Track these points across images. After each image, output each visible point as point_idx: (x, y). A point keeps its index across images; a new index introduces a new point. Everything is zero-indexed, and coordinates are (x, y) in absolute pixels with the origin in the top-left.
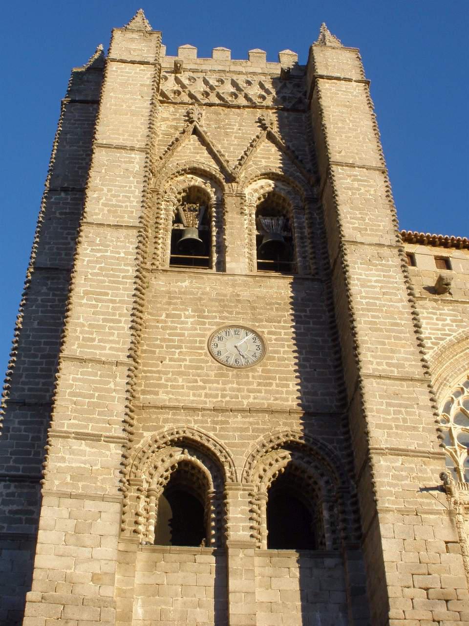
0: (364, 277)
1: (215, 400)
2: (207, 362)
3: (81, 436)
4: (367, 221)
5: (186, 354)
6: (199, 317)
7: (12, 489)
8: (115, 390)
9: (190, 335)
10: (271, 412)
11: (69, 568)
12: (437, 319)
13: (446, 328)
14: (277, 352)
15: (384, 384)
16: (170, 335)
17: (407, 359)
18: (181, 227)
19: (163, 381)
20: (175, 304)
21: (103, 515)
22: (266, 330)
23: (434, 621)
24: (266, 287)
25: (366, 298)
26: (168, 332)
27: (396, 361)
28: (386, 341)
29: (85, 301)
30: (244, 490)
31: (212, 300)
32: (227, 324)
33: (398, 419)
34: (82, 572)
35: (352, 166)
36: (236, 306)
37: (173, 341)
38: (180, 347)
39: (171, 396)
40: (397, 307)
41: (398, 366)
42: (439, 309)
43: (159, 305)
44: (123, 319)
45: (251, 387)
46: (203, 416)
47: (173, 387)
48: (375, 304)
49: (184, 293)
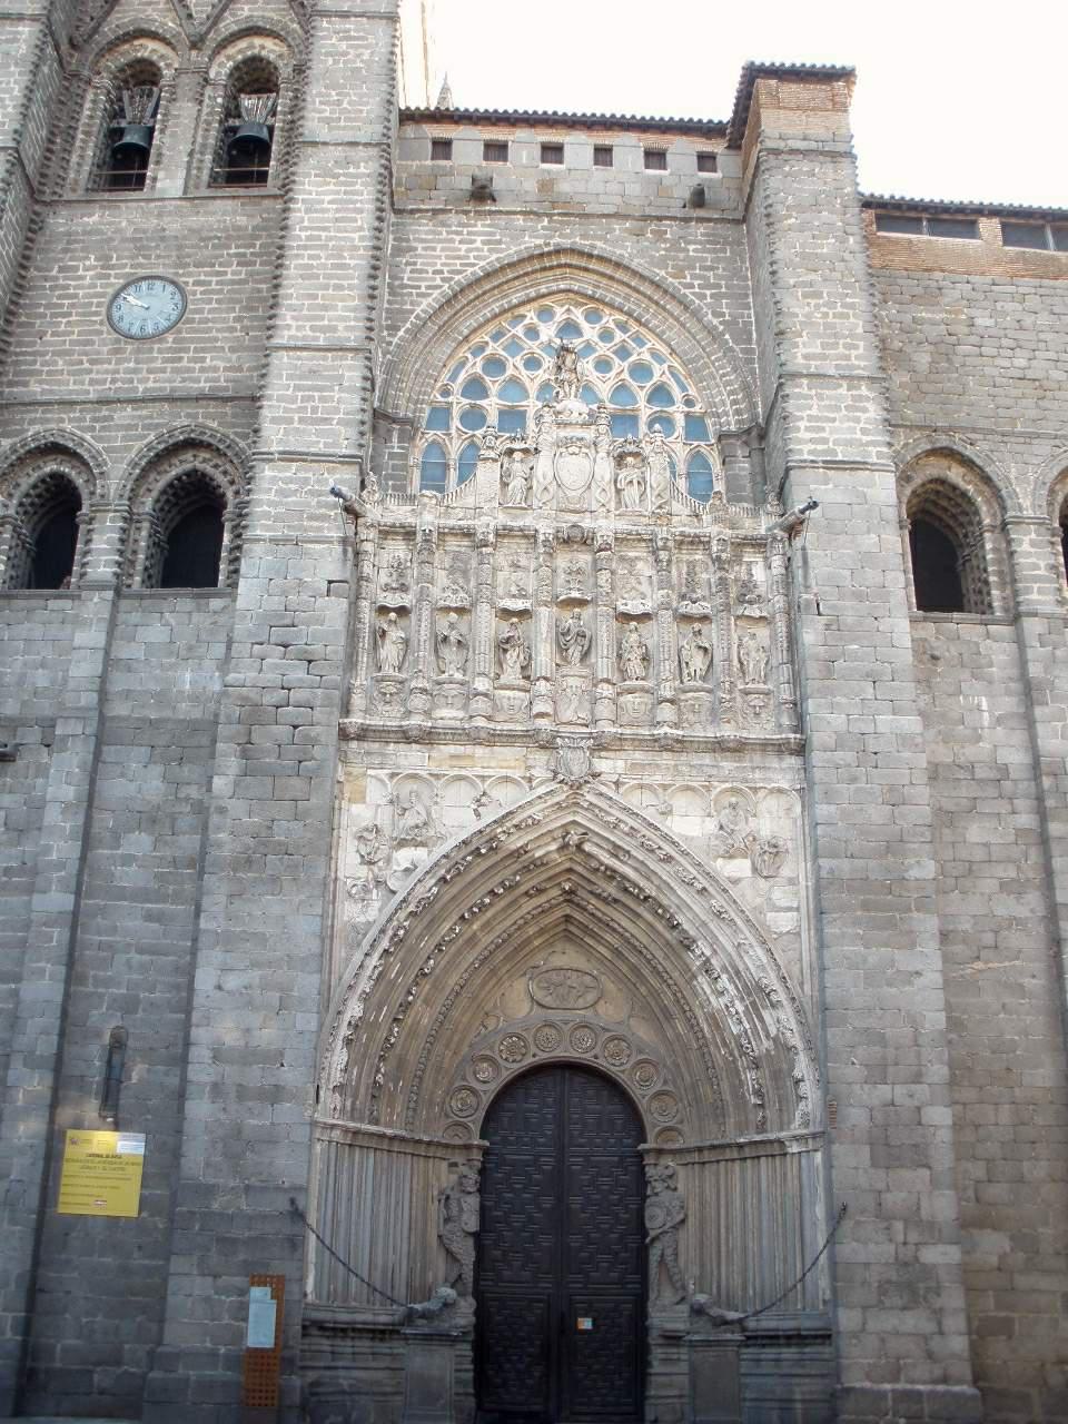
0: (314, 196)
1: (100, 388)
2: (101, 333)
4: (345, 105)
5: (78, 323)
6: (103, 267)
9: (85, 296)
10: (171, 399)
12: (460, 242)
13: (471, 255)
14: (200, 311)
15: (299, 358)
16: (59, 297)
18: (124, 124)
19: (38, 367)
20: (74, 250)
22: (191, 280)
23: (283, 688)
24: (207, 213)
25: (307, 229)
26: (57, 293)
27: (326, 322)
28: (320, 293)
30: (116, 511)
31: (124, 240)
32: (140, 275)
33: (306, 408)
35: (345, 15)
36: (157, 247)
37: (62, 306)
38: (65, 315)
39: (46, 387)
40: (353, 240)
41: (323, 329)
42: (464, 225)
43: (52, 255)
45: (153, 365)
46: (81, 411)
47: (49, 373)
48: (319, 238)
49: (89, 233)
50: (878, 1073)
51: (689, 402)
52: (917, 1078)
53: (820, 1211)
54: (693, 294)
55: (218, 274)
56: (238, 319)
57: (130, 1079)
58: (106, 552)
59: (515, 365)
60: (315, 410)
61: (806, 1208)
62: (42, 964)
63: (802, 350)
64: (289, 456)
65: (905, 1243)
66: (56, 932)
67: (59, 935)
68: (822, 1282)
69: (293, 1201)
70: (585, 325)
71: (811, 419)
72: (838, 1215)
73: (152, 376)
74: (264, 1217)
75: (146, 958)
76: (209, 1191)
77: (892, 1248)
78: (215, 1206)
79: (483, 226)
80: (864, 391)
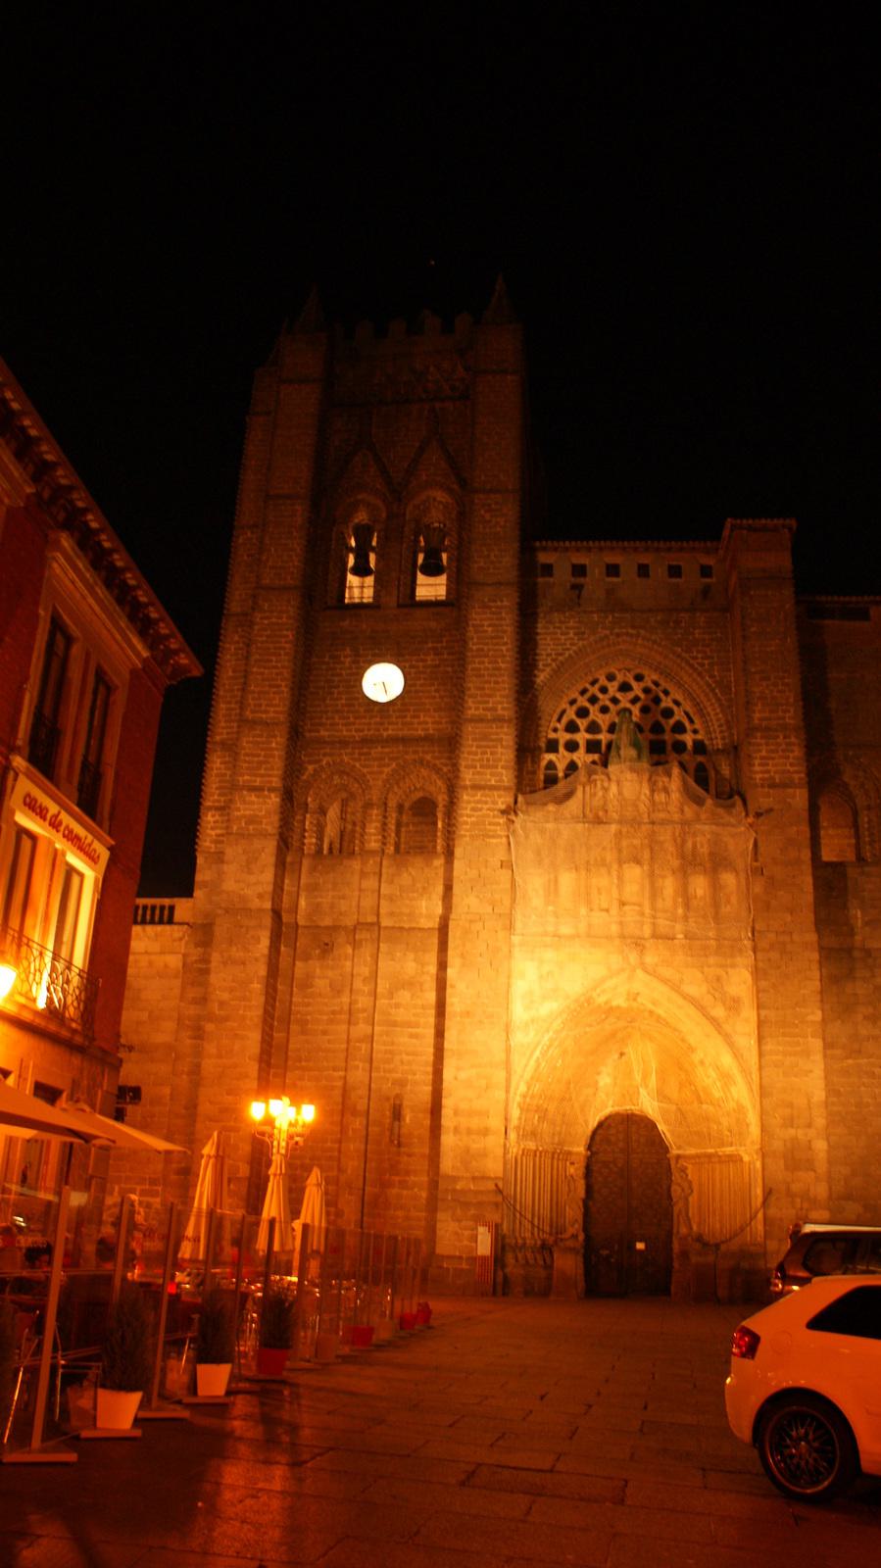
0: (479, 622)
1: (361, 734)
3: (253, 789)
6: (355, 656)
7: (217, 817)
8: (277, 749)
11: (243, 889)
12: (561, 634)
13: (568, 642)
17: (502, 703)
21: (266, 850)
26: (330, 673)
27: (491, 705)
28: (486, 686)
29: (255, 670)
34: (248, 892)
44: (283, 684)
47: (331, 725)
48: (483, 650)
50: (790, 1122)
51: (695, 732)
52: (809, 1126)
53: (759, 1191)
54: (698, 663)
55: (422, 660)
56: (436, 691)
57: (404, 1120)
58: (375, 835)
59: (594, 710)
60: (488, 760)
61: (753, 1189)
62: (356, 1063)
63: (757, 715)
64: (476, 787)
65: (801, 1209)
66: (364, 1046)
67: (364, 1047)
68: (759, 1226)
69: (496, 1185)
70: (634, 684)
71: (762, 758)
72: (768, 1194)
73: (390, 727)
74: (481, 1192)
75: (411, 1058)
76: (455, 1179)
77: (794, 1211)
78: (458, 1187)
79: (575, 622)
80: (793, 740)
